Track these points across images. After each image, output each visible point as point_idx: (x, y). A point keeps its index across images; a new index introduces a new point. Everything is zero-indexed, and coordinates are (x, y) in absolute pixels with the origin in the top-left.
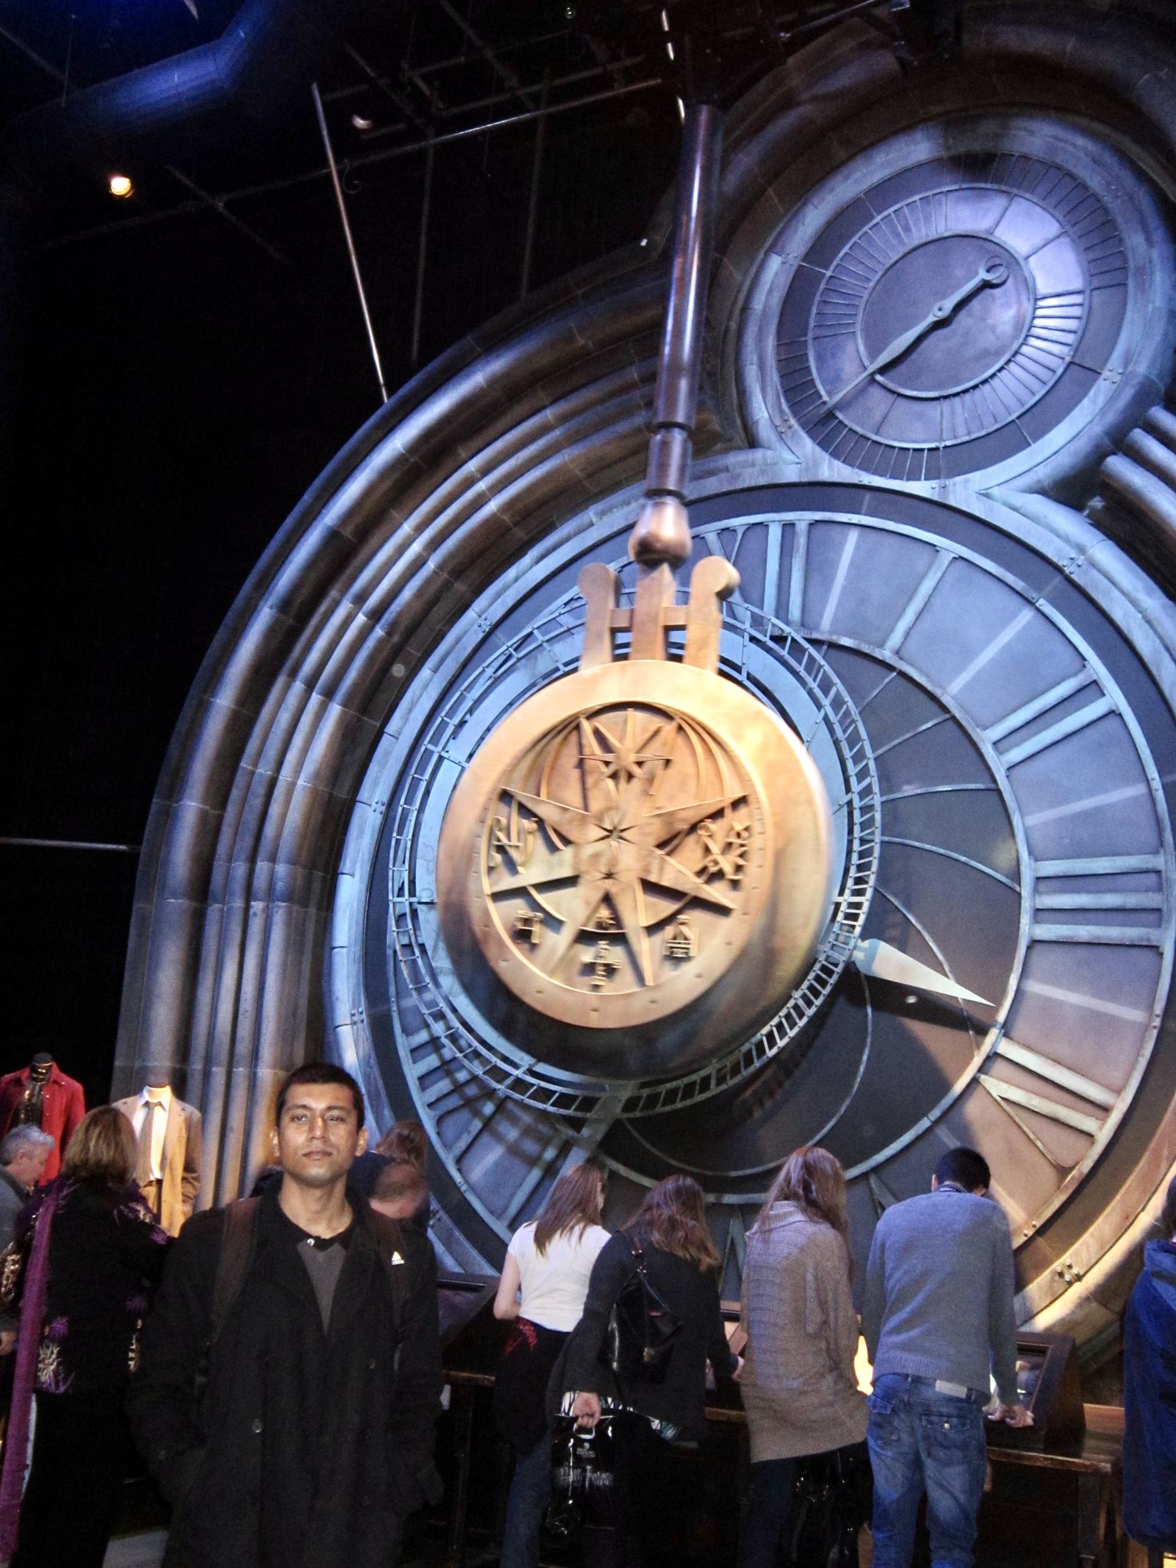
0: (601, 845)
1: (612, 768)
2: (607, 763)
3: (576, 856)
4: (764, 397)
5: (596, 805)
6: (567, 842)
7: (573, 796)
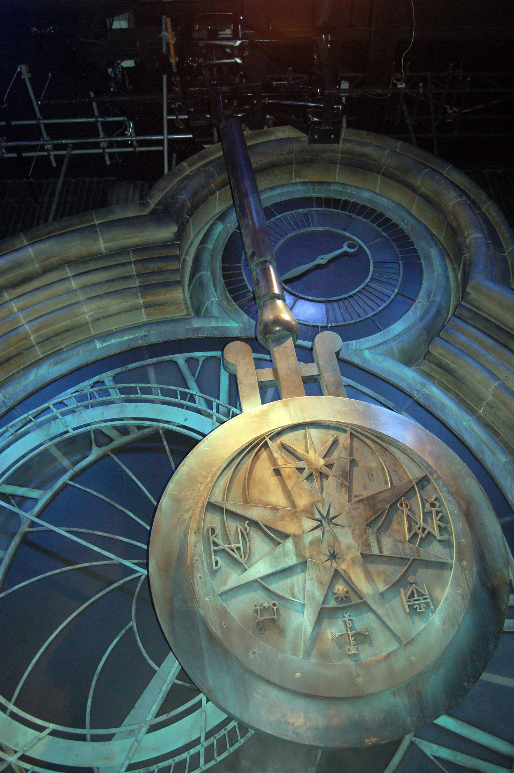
0: (318, 533)
1: (306, 472)
2: (301, 470)
3: (296, 545)
4: (215, 286)
5: (302, 502)
6: (286, 536)
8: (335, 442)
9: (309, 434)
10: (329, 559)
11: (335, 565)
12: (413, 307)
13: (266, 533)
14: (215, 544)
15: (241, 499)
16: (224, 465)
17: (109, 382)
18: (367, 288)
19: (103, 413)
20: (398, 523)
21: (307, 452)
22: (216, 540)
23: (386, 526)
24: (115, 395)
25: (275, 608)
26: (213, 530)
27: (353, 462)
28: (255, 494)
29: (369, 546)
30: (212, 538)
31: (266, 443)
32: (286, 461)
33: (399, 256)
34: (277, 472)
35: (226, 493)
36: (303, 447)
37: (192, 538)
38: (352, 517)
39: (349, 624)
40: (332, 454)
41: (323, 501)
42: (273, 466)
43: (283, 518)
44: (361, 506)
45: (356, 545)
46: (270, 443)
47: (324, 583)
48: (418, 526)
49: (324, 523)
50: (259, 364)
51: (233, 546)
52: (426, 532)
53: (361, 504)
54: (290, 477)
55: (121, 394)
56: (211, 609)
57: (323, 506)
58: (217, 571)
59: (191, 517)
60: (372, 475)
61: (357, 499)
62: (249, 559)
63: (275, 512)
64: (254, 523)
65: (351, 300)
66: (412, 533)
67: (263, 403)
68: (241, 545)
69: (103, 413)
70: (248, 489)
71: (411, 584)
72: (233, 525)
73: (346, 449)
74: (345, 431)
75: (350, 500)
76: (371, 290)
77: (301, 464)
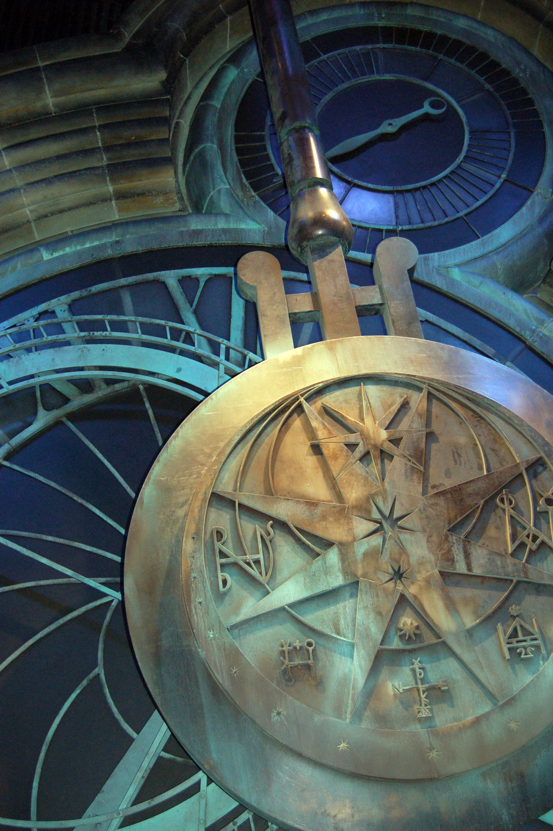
0: (376, 540)
1: (360, 450)
2: (352, 446)
3: (343, 557)
7: (316, 488)
8: (405, 405)
9: (366, 393)
10: (391, 579)
11: (400, 588)
12: (529, 203)
13: (298, 540)
14: (223, 555)
15: (262, 488)
16: (237, 438)
17: (62, 313)
18: (459, 171)
19: (53, 359)
20: (497, 528)
21: (362, 420)
22: (224, 549)
23: (479, 531)
24: (72, 332)
25: (311, 649)
26: (220, 534)
27: (430, 436)
28: (283, 481)
29: (452, 561)
30: (218, 545)
31: (300, 406)
32: (330, 432)
33: (510, 120)
34: (316, 449)
35: (239, 479)
36: (357, 411)
37: (188, 545)
38: (427, 517)
39: (420, 674)
40: (399, 424)
41: (384, 493)
42: (310, 440)
43: (324, 518)
44: (441, 501)
45: (433, 559)
46: (305, 405)
47: (384, 613)
48: (526, 532)
49: (385, 525)
50: (290, 286)
51: (250, 557)
52: (538, 542)
53: (442, 498)
54: (335, 457)
55: (81, 331)
56: (215, 649)
57: (385, 500)
58: (225, 594)
59: (186, 515)
60: (459, 455)
61: (435, 491)
62: (273, 577)
63: (312, 508)
64: (281, 525)
65: (433, 190)
66: (517, 543)
67: (296, 346)
68: (261, 556)
69: (53, 359)
70: (273, 475)
71: (514, 617)
72: (250, 528)
73: (420, 415)
74: (420, 389)
75: (424, 493)
76: (465, 175)
77: (352, 438)
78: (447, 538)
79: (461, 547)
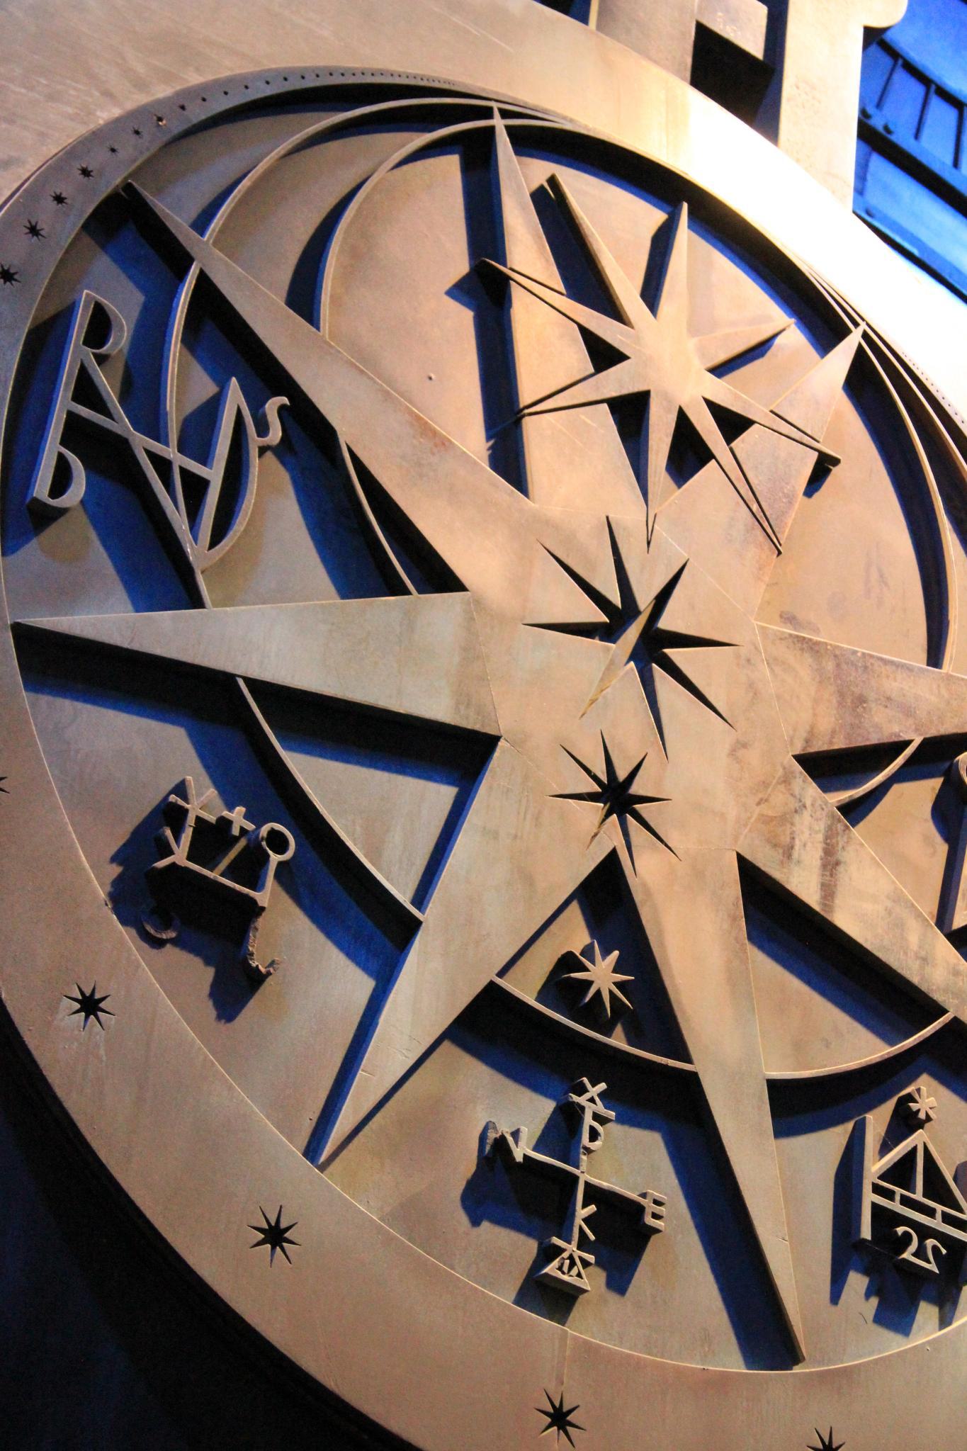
11: (611, 838)
45: (732, 813)
49: (632, 634)
53: (808, 659)
78: (786, 780)
79: (821, 826)
